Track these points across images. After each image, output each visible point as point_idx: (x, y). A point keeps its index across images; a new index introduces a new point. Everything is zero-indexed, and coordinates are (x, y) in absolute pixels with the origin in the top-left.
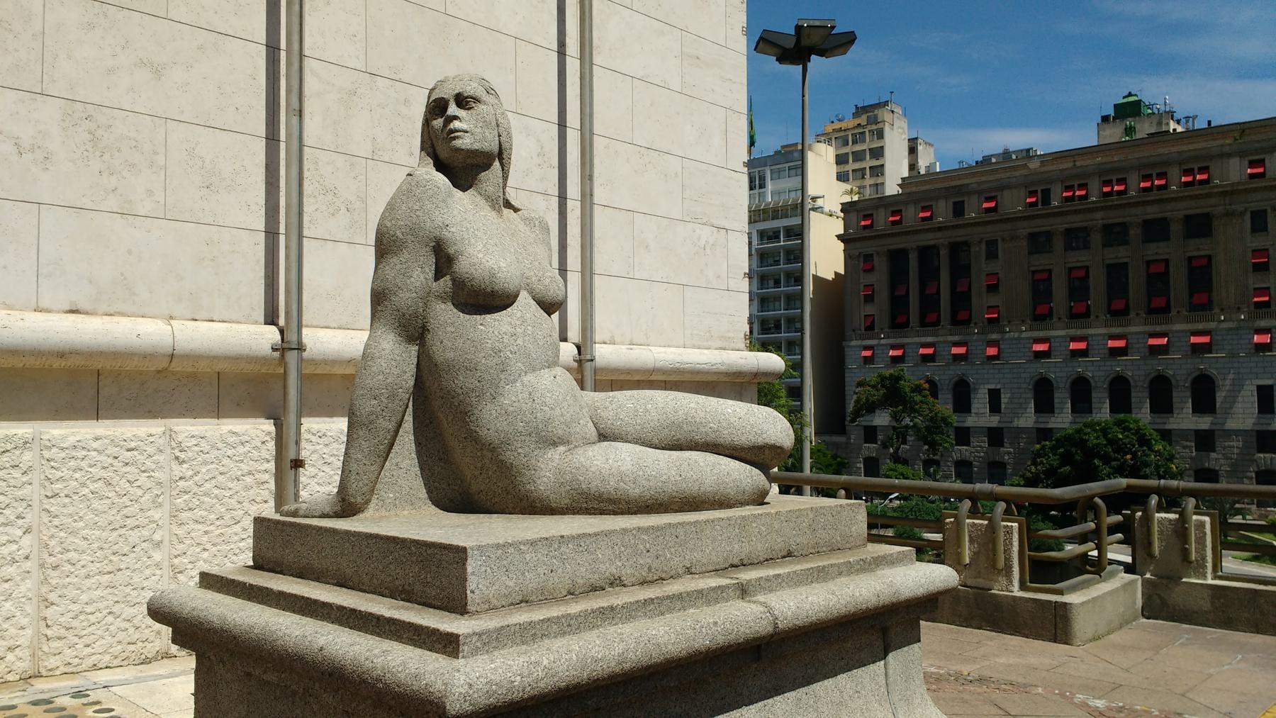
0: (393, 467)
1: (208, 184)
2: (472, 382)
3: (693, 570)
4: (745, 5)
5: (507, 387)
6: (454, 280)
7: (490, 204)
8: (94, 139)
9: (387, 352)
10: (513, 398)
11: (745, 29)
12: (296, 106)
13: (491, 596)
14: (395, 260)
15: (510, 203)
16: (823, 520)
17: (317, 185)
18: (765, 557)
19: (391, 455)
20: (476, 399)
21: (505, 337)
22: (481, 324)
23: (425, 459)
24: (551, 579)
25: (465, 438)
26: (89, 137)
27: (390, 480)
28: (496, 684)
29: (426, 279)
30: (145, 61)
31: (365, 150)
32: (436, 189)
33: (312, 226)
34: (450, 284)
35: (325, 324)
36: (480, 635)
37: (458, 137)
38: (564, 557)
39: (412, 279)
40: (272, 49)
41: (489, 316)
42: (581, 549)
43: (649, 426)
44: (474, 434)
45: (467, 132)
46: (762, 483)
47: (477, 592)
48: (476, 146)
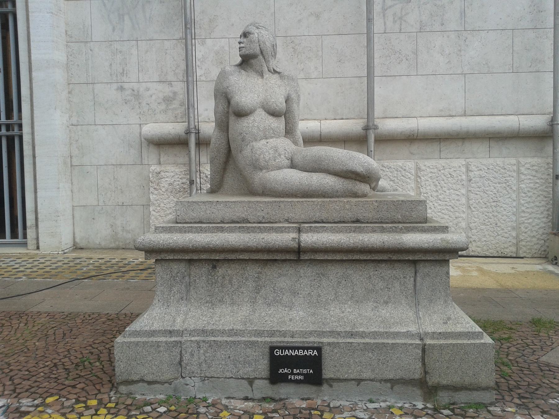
1: (339, 60)
3: (290, 221)
8: (295, 50)
10: (246, 152)
16: (386, 207)
18: (339, 220)
26: (293, 50)
28: (153, 241)
30: (312, 13)
33: (388, 70)
35: (396, 116)
36: (163, 227)
42: (227, 207)
45: (244, 47)
46: (350, 188)
47: (180, 216)
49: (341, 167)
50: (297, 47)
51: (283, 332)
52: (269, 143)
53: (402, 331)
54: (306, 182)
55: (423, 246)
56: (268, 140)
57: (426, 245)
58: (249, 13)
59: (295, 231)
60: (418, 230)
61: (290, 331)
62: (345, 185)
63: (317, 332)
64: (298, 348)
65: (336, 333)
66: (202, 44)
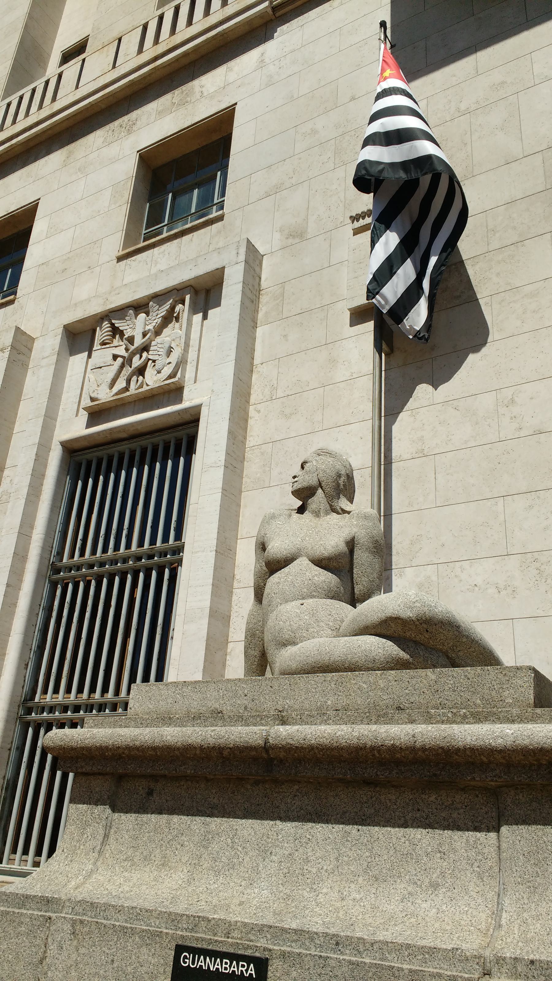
7: (315, 515)
8: (540, 572)
13: (139, 712)
15: (344, 510)
16: (452, 682)
24: (174, 707)
38: (185, 694)
42: (196, 690)
46: (395, 653)
47: (133, 709)
50: (543, 567)
51: (213, 922)
52: (305, 604)
53: (444, 947)
54: (327, 648)
55: (493, 744)
56: (304, 601)
57: (500, 741)
58: (467, 527)
59: (277, 723)
60: (499, 719)
61: (224, 921)
62: (387, 649)
63: (271, 930)
64: (222, 955)
65: (307, 936)
66: (400, 575)
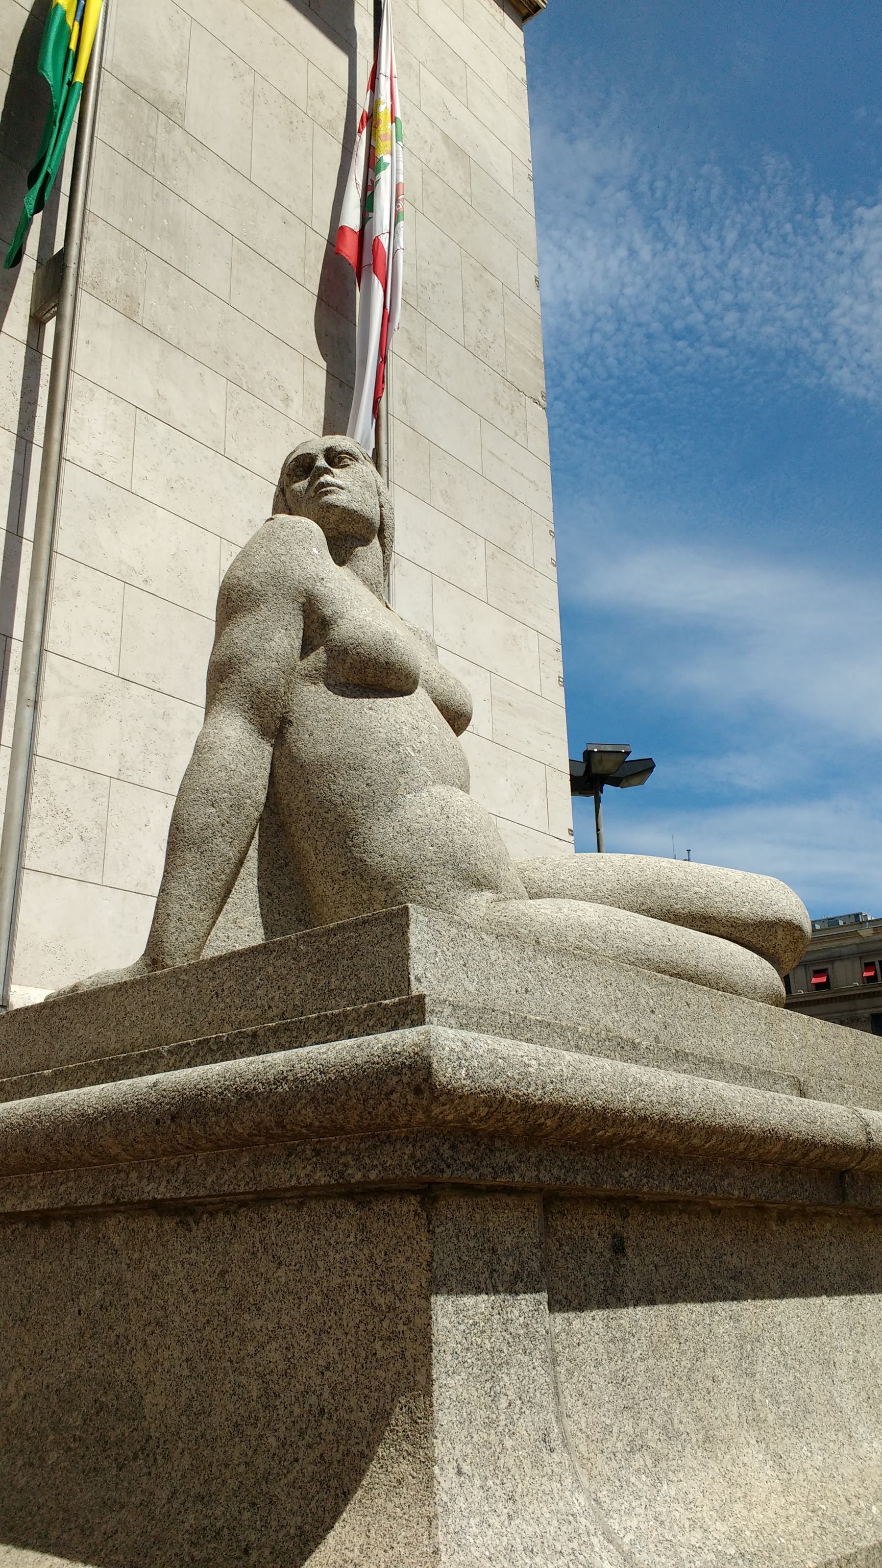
0: (229, 925)
2: (357, 786)
4: (560, 654)
5: (408, 796)
6: (329, 651)
9: (232, 740)
10: (419, 812)
11: (561, 680)
12: (31, 695)
14: (249, 618)
17: (45, 804)
19: (226, 907)
20: (364, 811)
21: (405, 727)
22: (370, 709)
23: (277, 917)
24: (526, 1003)
25: (344, 873)
27: (224, 944)
29: (292, 646)
31: (110, 766)
32: (308, 533)
34: (323, 657)
37: (330, 492)
38: (542, 975)
39: (273, 644)
40: (4, 638)
41: (381, 700)
43: (605, 889)
44: (360, 864)
45: (342, 489)
48: (354, 506)
49: (756, 908)
